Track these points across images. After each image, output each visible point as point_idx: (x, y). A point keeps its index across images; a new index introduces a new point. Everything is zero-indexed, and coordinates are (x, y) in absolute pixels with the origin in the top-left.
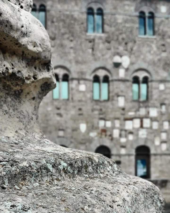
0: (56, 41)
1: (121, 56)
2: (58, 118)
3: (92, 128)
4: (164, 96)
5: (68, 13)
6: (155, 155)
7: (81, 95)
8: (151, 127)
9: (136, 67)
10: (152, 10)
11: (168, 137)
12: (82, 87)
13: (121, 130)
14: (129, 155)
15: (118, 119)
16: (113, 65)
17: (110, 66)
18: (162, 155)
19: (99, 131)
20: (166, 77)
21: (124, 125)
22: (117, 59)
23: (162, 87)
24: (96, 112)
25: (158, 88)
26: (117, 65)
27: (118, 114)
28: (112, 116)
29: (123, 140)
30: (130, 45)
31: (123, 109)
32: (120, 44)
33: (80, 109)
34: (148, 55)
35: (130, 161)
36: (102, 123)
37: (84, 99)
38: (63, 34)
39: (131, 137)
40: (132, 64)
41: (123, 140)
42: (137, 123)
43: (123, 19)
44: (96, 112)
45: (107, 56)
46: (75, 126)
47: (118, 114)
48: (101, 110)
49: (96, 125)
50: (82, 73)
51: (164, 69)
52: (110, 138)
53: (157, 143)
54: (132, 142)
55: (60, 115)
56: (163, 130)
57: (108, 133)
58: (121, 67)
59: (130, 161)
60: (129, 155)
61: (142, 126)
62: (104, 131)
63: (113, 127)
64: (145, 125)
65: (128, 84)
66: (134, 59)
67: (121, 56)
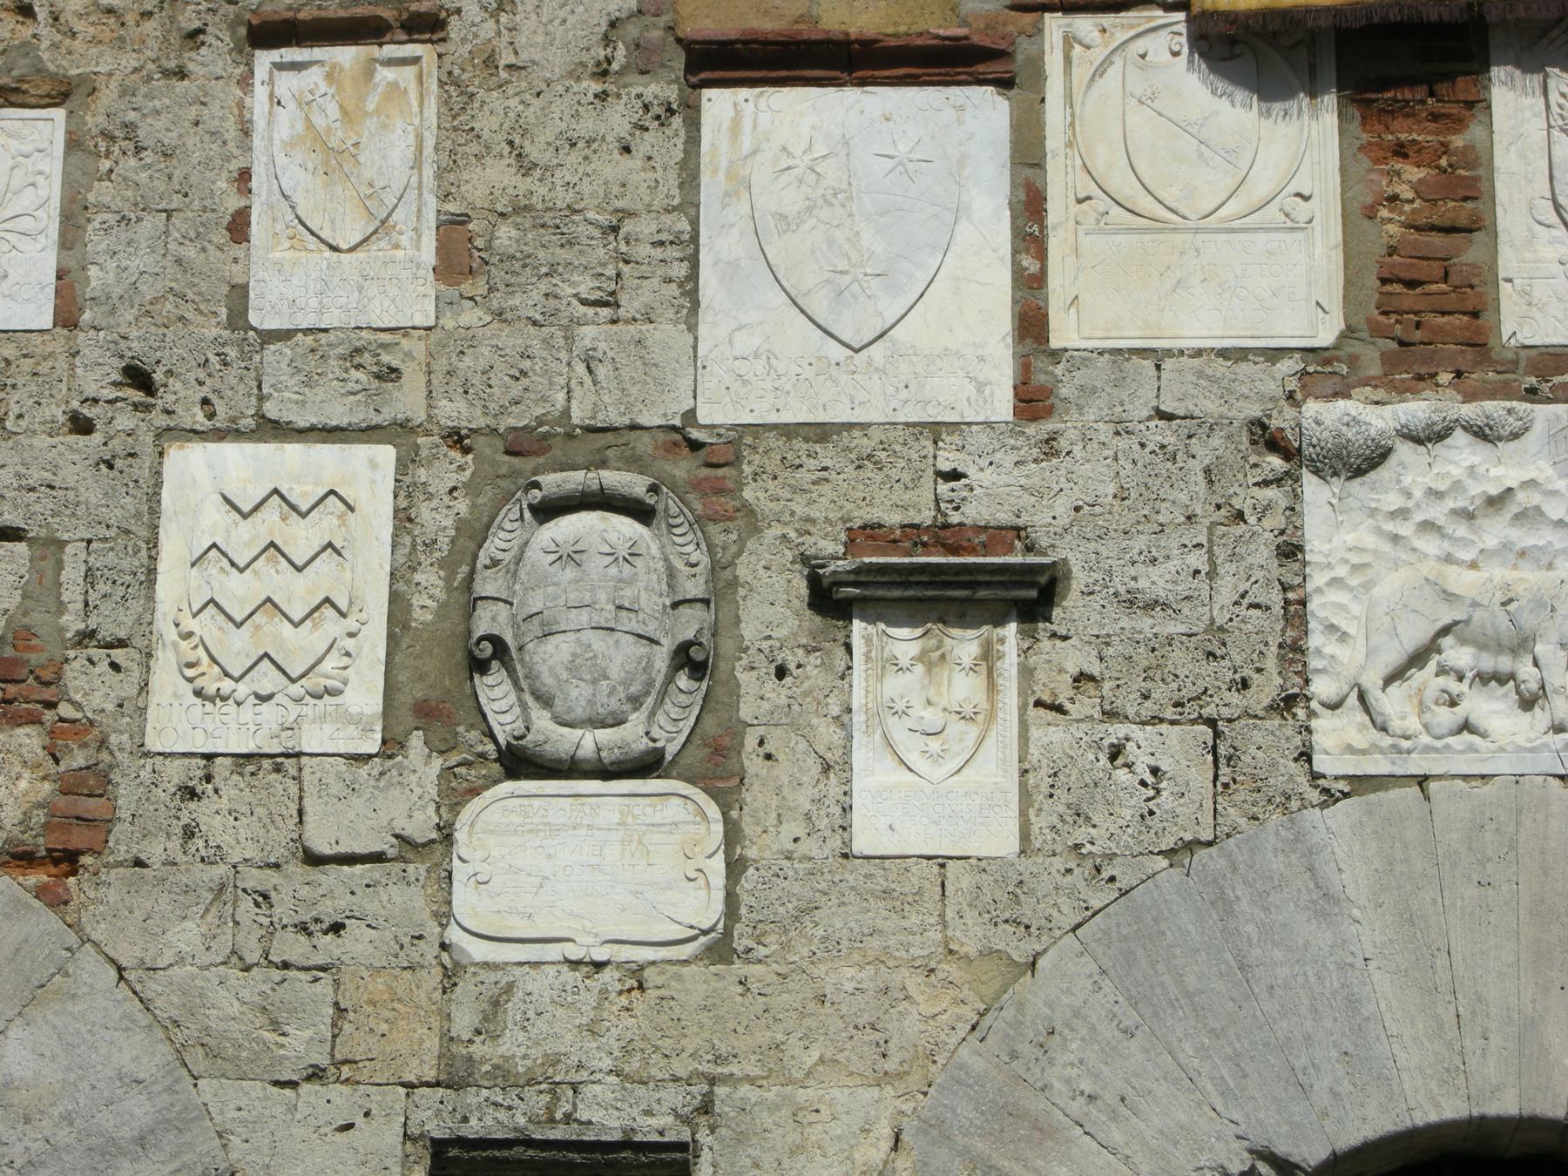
29: (578, 876)
39: (929, 754)
41: (578, 876)
54: (1000, 926)
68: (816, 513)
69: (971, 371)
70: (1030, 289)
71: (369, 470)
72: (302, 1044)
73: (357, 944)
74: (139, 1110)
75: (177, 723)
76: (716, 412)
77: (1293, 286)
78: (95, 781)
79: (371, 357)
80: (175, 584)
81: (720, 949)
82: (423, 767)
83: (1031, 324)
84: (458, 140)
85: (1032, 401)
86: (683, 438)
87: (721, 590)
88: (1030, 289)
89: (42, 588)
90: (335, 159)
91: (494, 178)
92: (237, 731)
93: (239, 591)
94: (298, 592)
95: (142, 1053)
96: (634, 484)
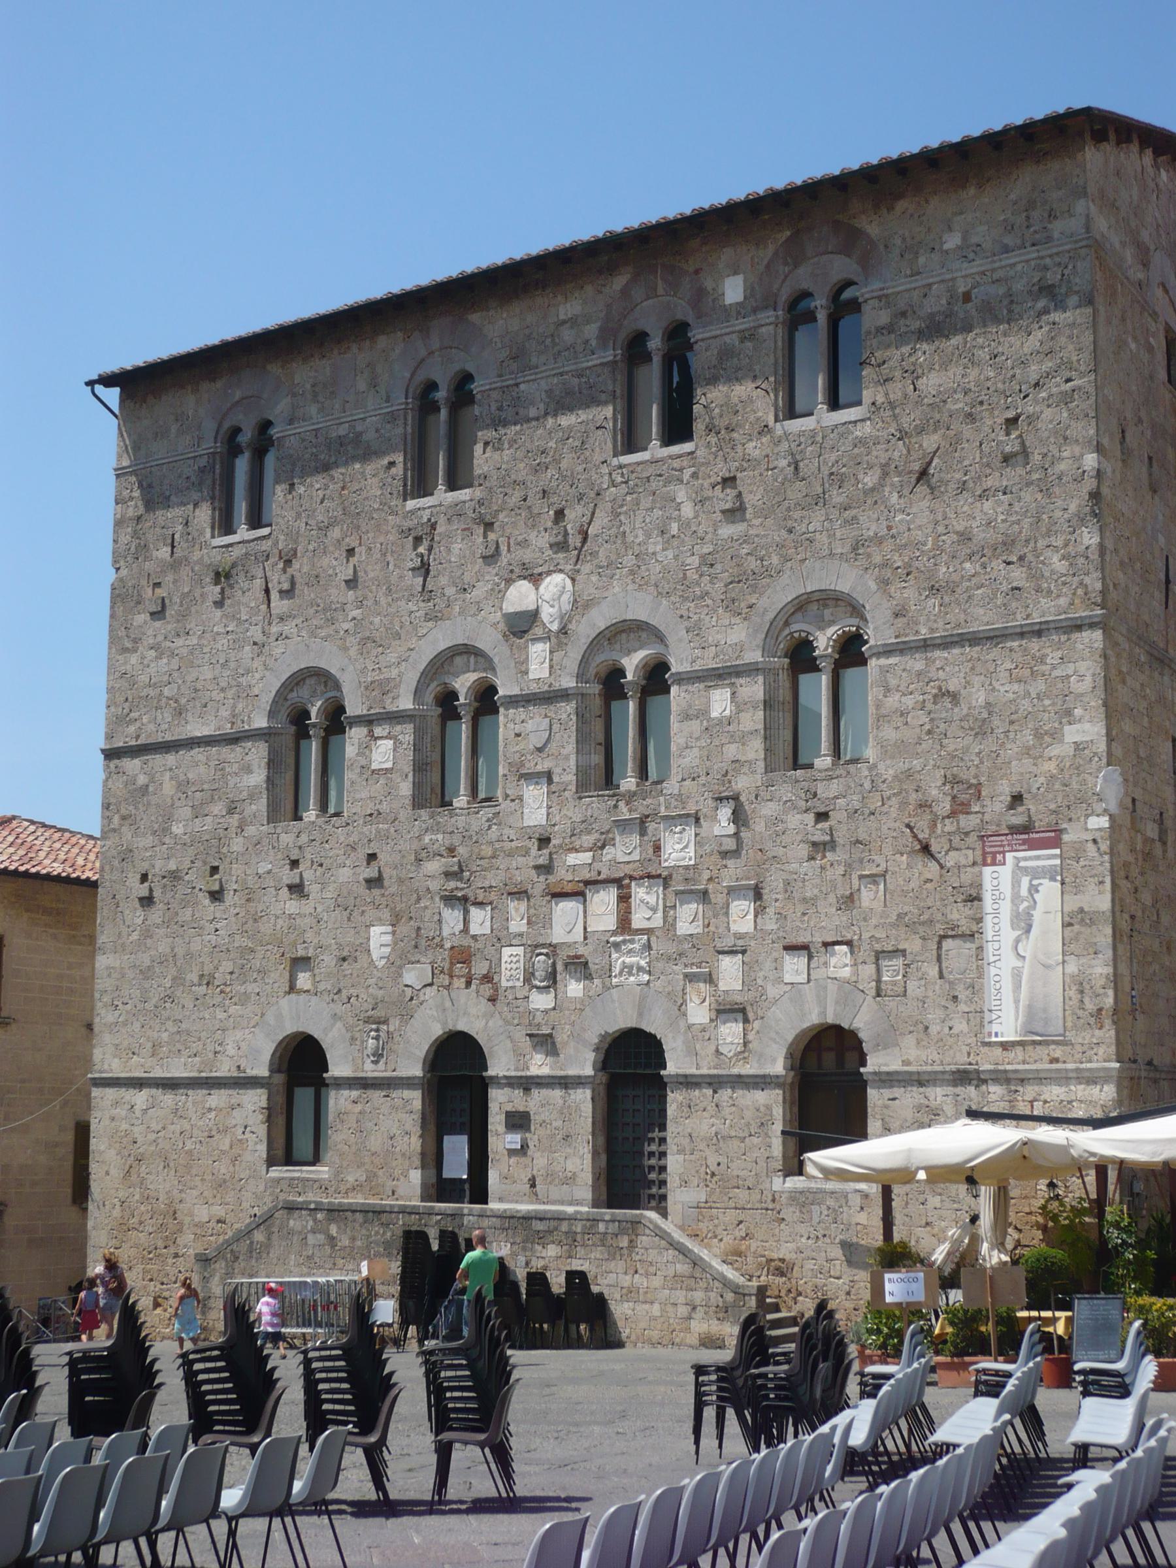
0: (296, 565)
1: (535, 579)
2: (293, 906)
3: (415, 943)
4: (731, 751)
5: (343, 430)
6: (688, 1082)
7: (379, 787)
8: (669, 925)
9: (600, 619)
10: (683, 311)
11: (748, 982)
12: (383, 754)
13: (534, 948)
14: (566, 1083)
15: (520, 894)
16: (502, 626)
17: (489, 639)
18: (716, 1083)
19: (442, 958)
20: (740, 647)
21: (548, 922)
22: (520, 596)
23: (720, 702)
24: (434, 866)
25: (704, 713)
26: (522, 625)
27: (522, 868)
28: (493, 879)
30: (574, 515)
31: (544, 841)
32: (533, 519)
33: (372, 857)
34: (655, 545)
35: (566, 1113)
36: (452, 918)
37: (384, 808)
38: (324, 529)
40: (580, 605)
41: (541, 1001)
42: (603, 906)
43: (549, 392)
44: (434, 866)
45: (480, 592)
46: (350, 937)
47: (522, 868)
48: (451, 850)
49: (429, 931)
50: (385, 688)
51: (730, 604)
52: (487, 990)
53: (698, 1013)
54: (580, 1007)
55: (297, 889)
56: (728, 943)
57: (480, 968)
58: (538, 631)
59: (566, 1113)
60: (566, 1083)
61: (624, 924)
62: (462, 956)
63: (500, 938)
64: (639, 919)
65: (567, 710)
66: (590, 582)
67: (535, 579)
68: (563, 954)
69: (578, 935)
70: (585, 922)
71: (520, 950)
72: (516, 1022)
73: (521, 1009)
74: (502, 1030)
75: (504, 984)
76: (554, 942)
77: (609, 922)
78: (496, 990)
79: (521, 935)
80: (503, 966)
81: (554, 1009)
82: (527, 987)
83: (585, 928)
84: (529, 907)
85: (585, 938)
86: (550, 945)
87: (554, 964)
88: (585, 922)
89: (490, 967)
90: (517, 910)
91: (532, 911)
92: (510, 984)
93: (509, 967)
94: (514, 966)
95: (501, 1023)
96: (544, 951)
